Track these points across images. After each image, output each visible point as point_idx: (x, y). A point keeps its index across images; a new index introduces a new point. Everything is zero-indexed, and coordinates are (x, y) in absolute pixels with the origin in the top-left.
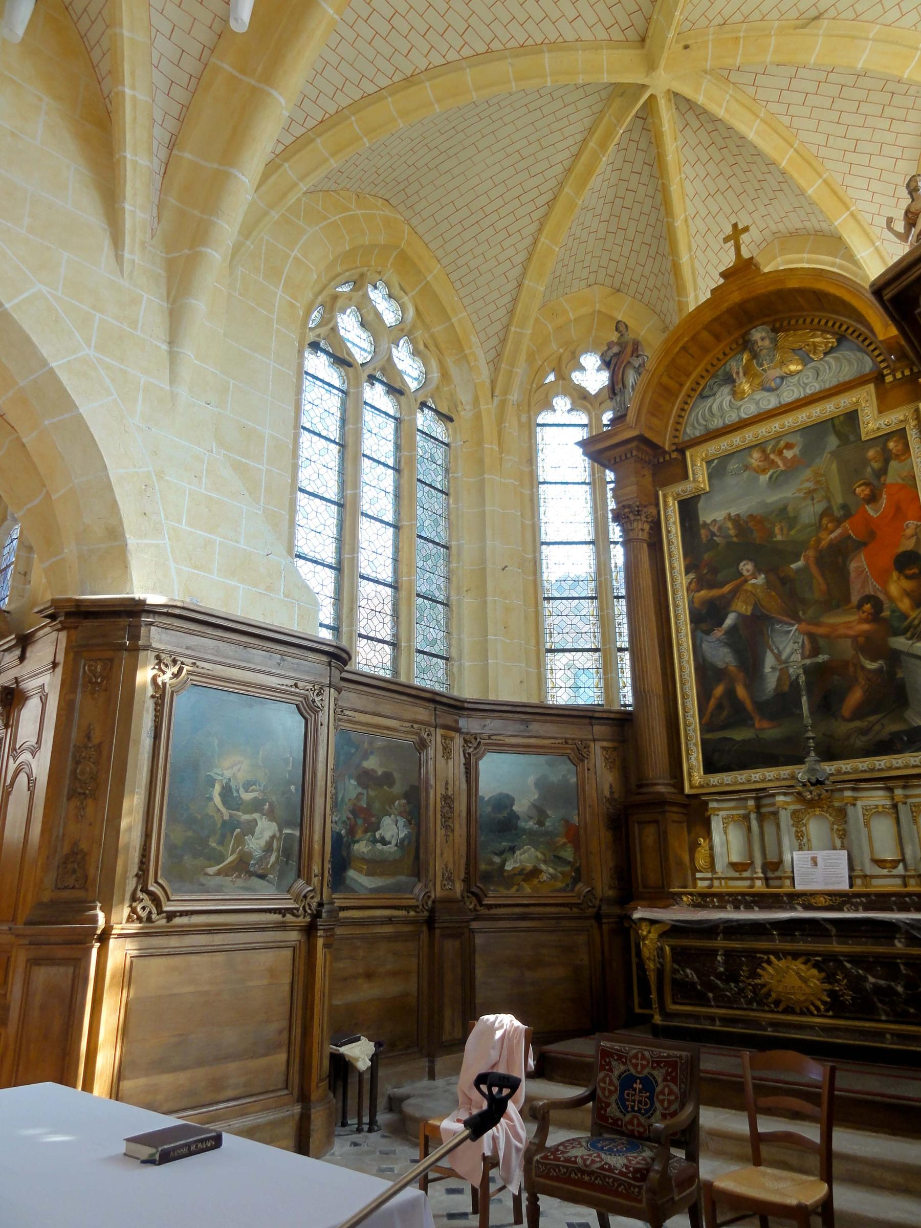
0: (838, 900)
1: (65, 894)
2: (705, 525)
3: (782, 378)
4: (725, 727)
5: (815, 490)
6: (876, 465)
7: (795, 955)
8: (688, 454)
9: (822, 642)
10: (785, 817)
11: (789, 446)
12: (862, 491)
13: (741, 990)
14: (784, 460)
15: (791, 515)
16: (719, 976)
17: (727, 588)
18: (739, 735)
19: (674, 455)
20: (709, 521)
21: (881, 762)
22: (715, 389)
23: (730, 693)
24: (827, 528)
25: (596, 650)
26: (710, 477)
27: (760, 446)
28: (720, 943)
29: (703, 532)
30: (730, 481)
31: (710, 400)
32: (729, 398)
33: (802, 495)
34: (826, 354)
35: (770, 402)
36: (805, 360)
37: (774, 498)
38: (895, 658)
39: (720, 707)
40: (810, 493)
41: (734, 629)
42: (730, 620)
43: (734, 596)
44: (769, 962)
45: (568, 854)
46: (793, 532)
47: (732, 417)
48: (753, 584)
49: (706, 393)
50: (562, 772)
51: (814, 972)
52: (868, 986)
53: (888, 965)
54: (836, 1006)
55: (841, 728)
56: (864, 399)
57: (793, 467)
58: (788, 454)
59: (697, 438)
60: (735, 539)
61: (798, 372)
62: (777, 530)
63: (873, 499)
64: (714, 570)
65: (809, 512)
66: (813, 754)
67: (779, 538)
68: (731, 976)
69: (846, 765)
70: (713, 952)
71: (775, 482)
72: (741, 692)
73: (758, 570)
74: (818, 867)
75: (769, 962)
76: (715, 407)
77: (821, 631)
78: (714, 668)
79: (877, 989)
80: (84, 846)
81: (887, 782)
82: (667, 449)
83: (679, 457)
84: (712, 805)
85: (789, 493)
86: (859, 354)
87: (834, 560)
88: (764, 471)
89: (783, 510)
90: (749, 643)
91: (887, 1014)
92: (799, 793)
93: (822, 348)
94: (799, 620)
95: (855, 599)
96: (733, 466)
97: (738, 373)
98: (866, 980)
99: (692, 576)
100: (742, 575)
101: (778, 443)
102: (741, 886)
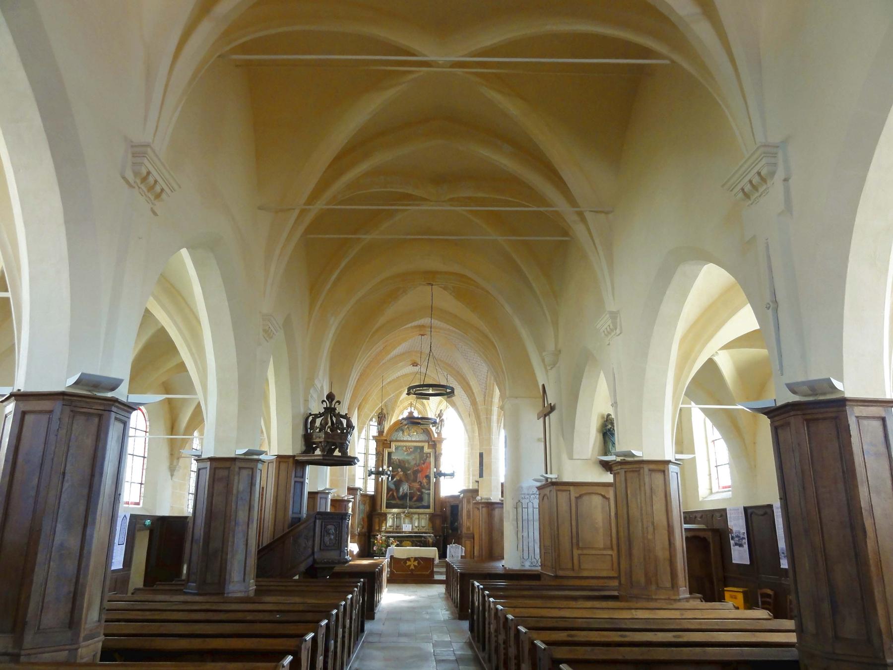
0: (410, 532)
18: (393, 502)
35: (410, 439)
38: (422, 493)
53: (420, 542)
55: (412, 503)
56: (426, 445)
57: (411, 453)
65: (413, 463)
74: (407, 527)
81: (419, 514)
85: (409, 458)
87: (416, 473)
89: (408, 462)
90: (398, 484)
101: (409, 448)
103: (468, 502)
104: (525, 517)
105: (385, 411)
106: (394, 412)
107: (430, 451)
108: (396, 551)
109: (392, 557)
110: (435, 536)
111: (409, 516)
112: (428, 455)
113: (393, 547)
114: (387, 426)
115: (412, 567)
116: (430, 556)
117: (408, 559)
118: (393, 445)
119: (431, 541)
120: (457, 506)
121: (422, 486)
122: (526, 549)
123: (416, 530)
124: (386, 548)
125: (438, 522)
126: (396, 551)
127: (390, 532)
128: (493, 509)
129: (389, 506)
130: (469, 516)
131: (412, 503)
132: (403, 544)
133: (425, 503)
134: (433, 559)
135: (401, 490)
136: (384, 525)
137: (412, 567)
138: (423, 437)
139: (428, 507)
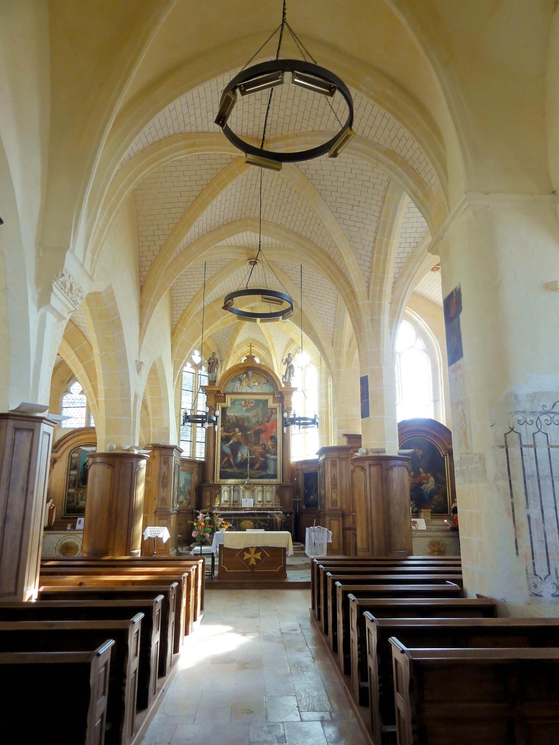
1: (163, 506)
2: (228, 416)
4: (226, 468)
7: (249, 520)
11: (251, 403)
17: (231, 434)
21: (261, 480)
23: (229, 460)
25: (191, 441)
27: (245, 400)
28: (233, 518)
35: (249, 390)
36: (259, 384)
37: (246, 414)
38: (267, 458)
39: (225, 463)
40: (255, 416)
41: (232, 444)
42: (231, 442)
45: (188, 497)
47: (239, 391)
50: (188, 477)
53: (265, 521)
55: (253, 472)
56: (270, 398)
57: (252, 408)
58: (251, 405)
63: (268, 422)
64: (229, 428)
65: (254, 420)
69: (254, 481)
71: (247, 410)
72: (231, 460)
73: (240, 431)
74: (247, 502)
77: (252, 449)
78: (225, 453)
80: (165, 497)
81: (263, 485)
85: (250, 414)
87: (258, 433)
88: (245, 407)
89: (248, 418)
90: (235, 449)
95: (261, 443)
96: (237, 403)
102: (227, 506)
103: (334, 465)
104: (530, 468)
105: (217, 356)
106: (229, 357)
107: (276, 405)
108: (228, 537)
109: (221, 546)
110: (285, 513)
111: (250, 488)
112: (273, 411)
113: (223, 532)
114: (220, 374)
115: (253, 562)
116: (281, 544)
117: (247, 550)
118: (228, 398)
119: (279, 519)
120: (316, 474)
121: (266, 451)
122: (539, 550)
123: (259, 506)
124: (212, 533)
125: (288, 495)
126: (228, 537)
127: (225, 509)
128: (391, 468)
129: (224, 475)
130: (334, 486)
131: (253, 472)
132: (243, 524)
133: (270, 472)
134: (285, 550)
135: (239, 455)
136: (217, 500)
137: (253, 562)
138: (266, 388)
139: (275, 476)
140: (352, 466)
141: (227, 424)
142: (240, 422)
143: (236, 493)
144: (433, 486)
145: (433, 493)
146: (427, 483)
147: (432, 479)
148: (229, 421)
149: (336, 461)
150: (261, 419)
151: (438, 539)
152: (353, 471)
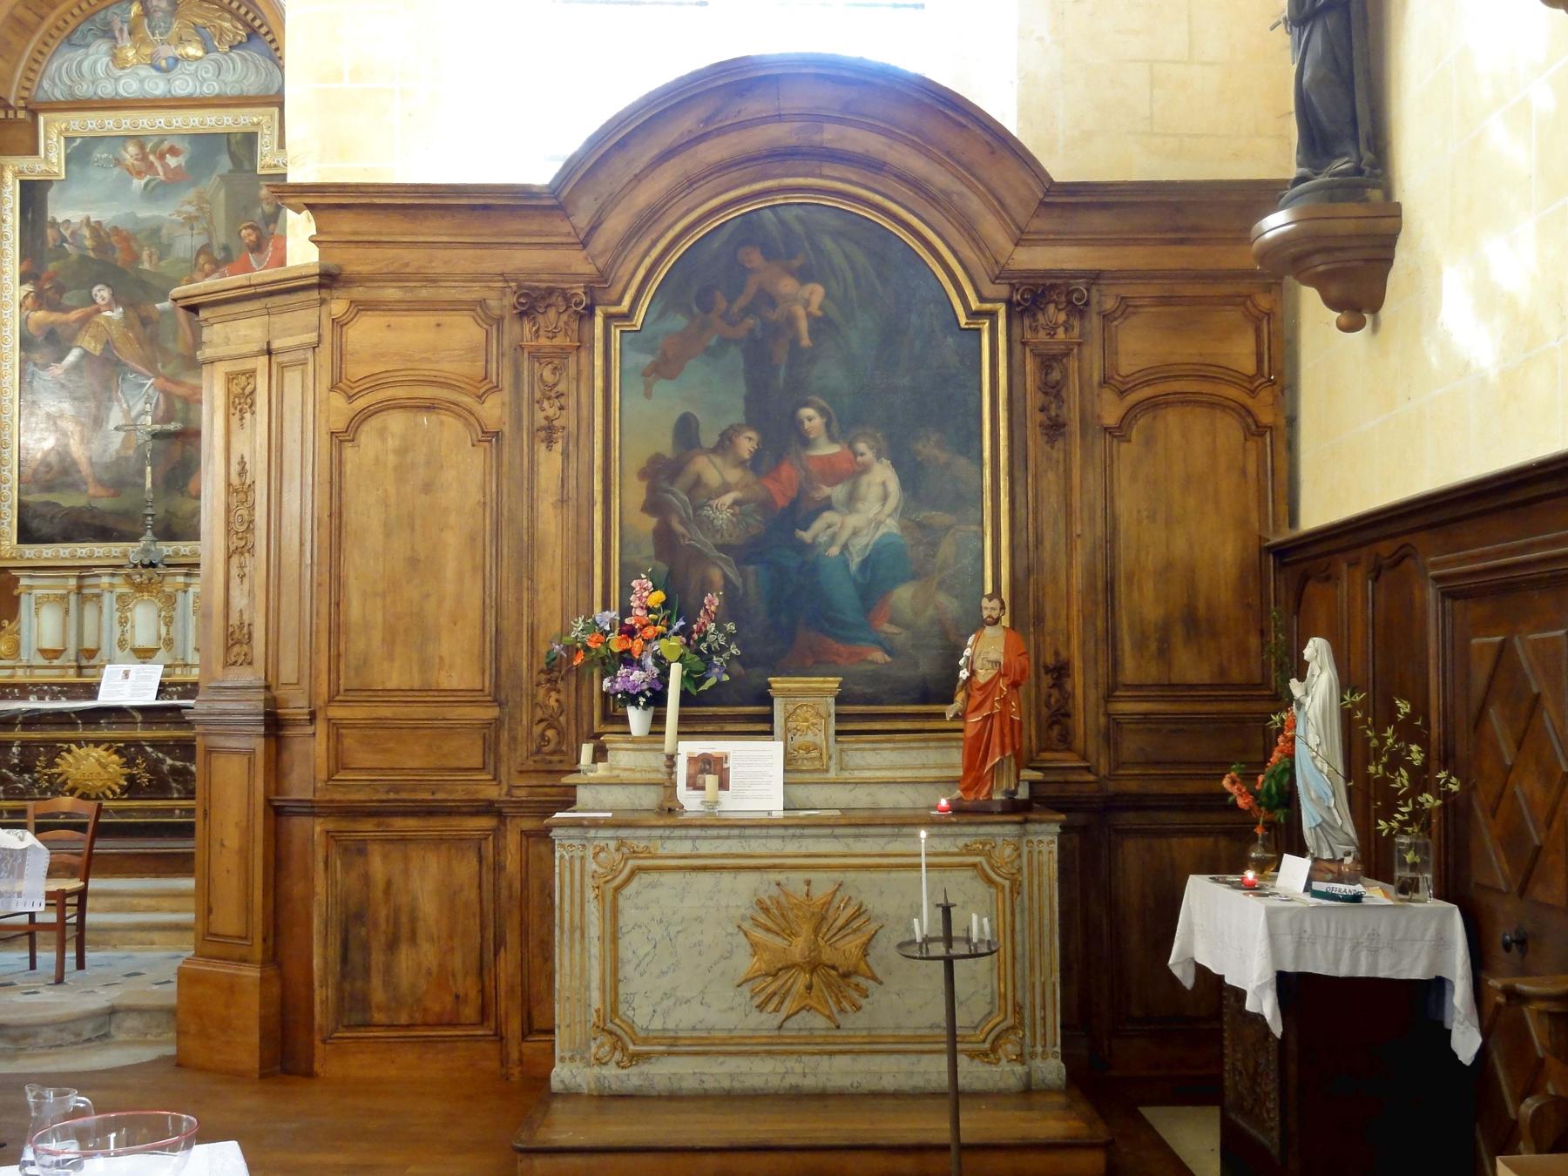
2: (54, 224)
3: (176, 60)
5: (196, 218)
6: (268, 209)
7: (97, 743)
8: (41, 118)
9: (178, 405)
10: (107, 599)
11: (173, 151)
12: (248, 235)
13: (36, 781)
14: (166, 166)
15: (165, 241)
16: (12, 768)
19: (21, 115)
20: (60, 220)
22: (89, 39)
24: (202, 270)
26: (68, 159)
27: (140, 140)
28: (18, 734)
29: (50, 232)
30: (95, 173)
31: (81, 51)
32: (106, 59)
33: (180, 219)
34: (231, 47)
35: (157, 87)
37: (146, 212)
40: (190, 220)
43: (80, 329)
44: (69, 751)
46: (163, 263)
47: (106, 90)
48: (108, 318)
49: (76, 39)
51: (115, 757)
52: (165, 768)
54: (132, 788)
58: (172, 161)
59: (59, 102)
60: (92, 254)
61: (197, 59)
62: (145, 254)
64: (61, 289)
65: (186, 243)
66: (149, 533)
67: (146, 266)
68: (26, 767)
70: (7, 745)
73: (116, 300)
75: (69, 751)
76: (86, 66)
77: (179, 391)
79: (173, 769)
82: (12, 102)
83: (29, 119)
84: (23, 582)
85: (165, 212)
86: (269, 63)
88: (139, 174)
89: (155, 232)
91: (179, 792)
92: (128, 575)
93: (229, 37)
94: (157, 375)
96: (100, 154)
97: (121, 30)
98: (163, 761)
99: (28, 288)
100: (94, 302)
118: (53, 132)
140: (338, 400)
141: (52, 267)
142: (119, 256)
143: (90, 612)
144: (891, 526)
145: (878, 573)
146: (852, 499)
147: (882, 477)
148: (60, 252)
149: (251, 374)
150: (221, 237)
151: (823, 884)
152: (342, 438)
